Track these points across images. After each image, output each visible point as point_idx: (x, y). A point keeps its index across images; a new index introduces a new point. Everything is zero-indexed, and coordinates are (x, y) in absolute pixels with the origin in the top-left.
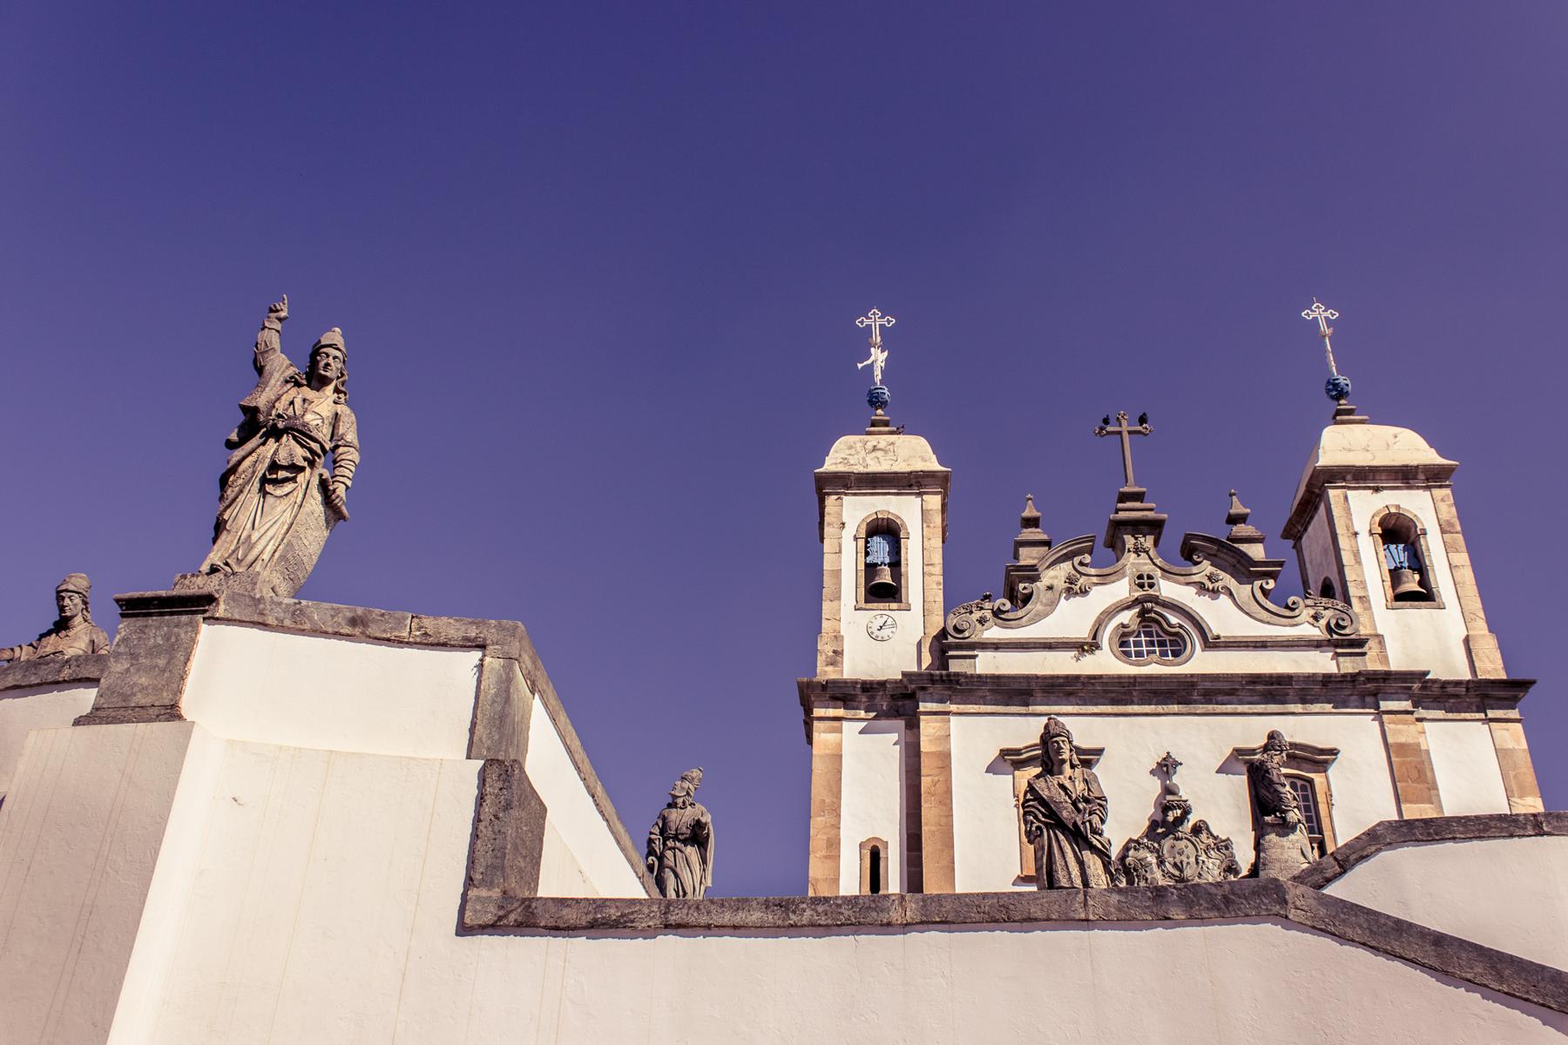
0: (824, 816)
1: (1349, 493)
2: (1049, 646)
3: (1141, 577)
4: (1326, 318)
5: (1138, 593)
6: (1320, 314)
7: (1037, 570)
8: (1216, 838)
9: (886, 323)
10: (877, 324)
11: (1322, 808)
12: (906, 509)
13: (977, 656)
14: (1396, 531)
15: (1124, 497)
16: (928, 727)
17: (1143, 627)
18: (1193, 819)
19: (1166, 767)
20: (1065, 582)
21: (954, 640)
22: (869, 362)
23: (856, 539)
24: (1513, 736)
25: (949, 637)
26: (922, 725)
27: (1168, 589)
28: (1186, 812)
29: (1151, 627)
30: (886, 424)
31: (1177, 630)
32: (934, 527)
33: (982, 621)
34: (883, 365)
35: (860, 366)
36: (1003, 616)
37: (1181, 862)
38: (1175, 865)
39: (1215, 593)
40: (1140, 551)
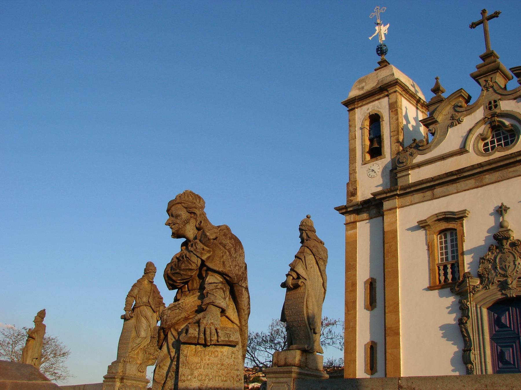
0: (350, 271)
2: (443, 158)
3: (490, 103)
7: (434, 118)
9: (382, 11)
10: (379, 13)
13: (409, 174)
16: (387, 218)
17: (495, 132)
20: (451, 120)
21: (400, 168)
23: (361, 129)
25: (397, 168)
26: (384, 216)
29: (500, 130)
31: (510, 128)
32: (395, 110)
33: (411, 155)
34: (386, 32)
35: (370, 38)
36: (420, 148)
37: (505, 266)
38: (502, 268)
40: (489, 88)
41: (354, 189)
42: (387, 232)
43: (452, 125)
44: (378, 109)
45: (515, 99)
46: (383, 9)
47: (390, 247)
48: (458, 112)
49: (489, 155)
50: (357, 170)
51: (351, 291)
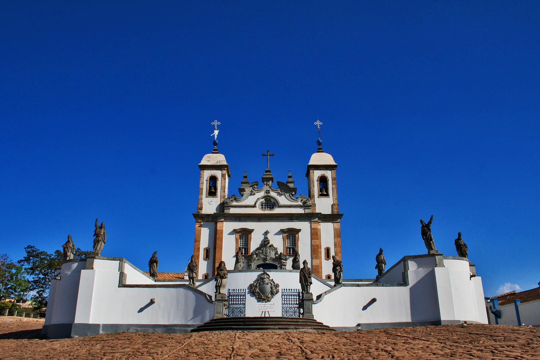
1: (315, 171)
3: (267, 191)
4: (320, 124)
5: (266, 195)
6: (318, 123)
8: (274, 247)
11: (297, 241)
12: (218, 173)
14: (323, 180)
15: (266, 172)
16: (219, 225)
18: (270, 244)
19: (266, 233)
22: (214, 134)
23: (207, 181)
24: (337, 225)
26: (218, 224)
27: (273, 194)
28: (269, 243)
30: (217, 150)
33: (232, 201)
35: (211, 135)
38: (265, 253)
39: (282, 194)
41: (201, 207)
42: (218, 230)
43: (251, 194)
44: (216, 174)
45: (276, 193)
46: (219, 123)
47: (219, 236)
48: (254, 190)
49: (264, 210)
50: (203, 199)
51: (197, 251)
